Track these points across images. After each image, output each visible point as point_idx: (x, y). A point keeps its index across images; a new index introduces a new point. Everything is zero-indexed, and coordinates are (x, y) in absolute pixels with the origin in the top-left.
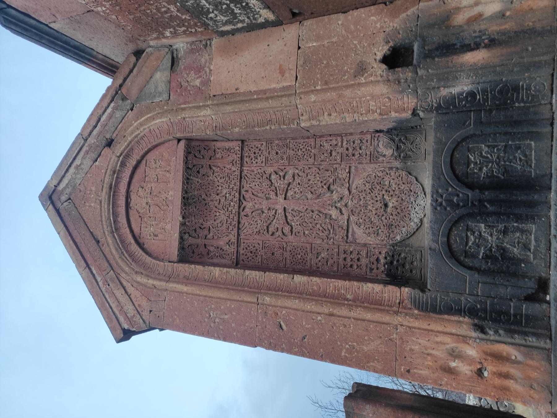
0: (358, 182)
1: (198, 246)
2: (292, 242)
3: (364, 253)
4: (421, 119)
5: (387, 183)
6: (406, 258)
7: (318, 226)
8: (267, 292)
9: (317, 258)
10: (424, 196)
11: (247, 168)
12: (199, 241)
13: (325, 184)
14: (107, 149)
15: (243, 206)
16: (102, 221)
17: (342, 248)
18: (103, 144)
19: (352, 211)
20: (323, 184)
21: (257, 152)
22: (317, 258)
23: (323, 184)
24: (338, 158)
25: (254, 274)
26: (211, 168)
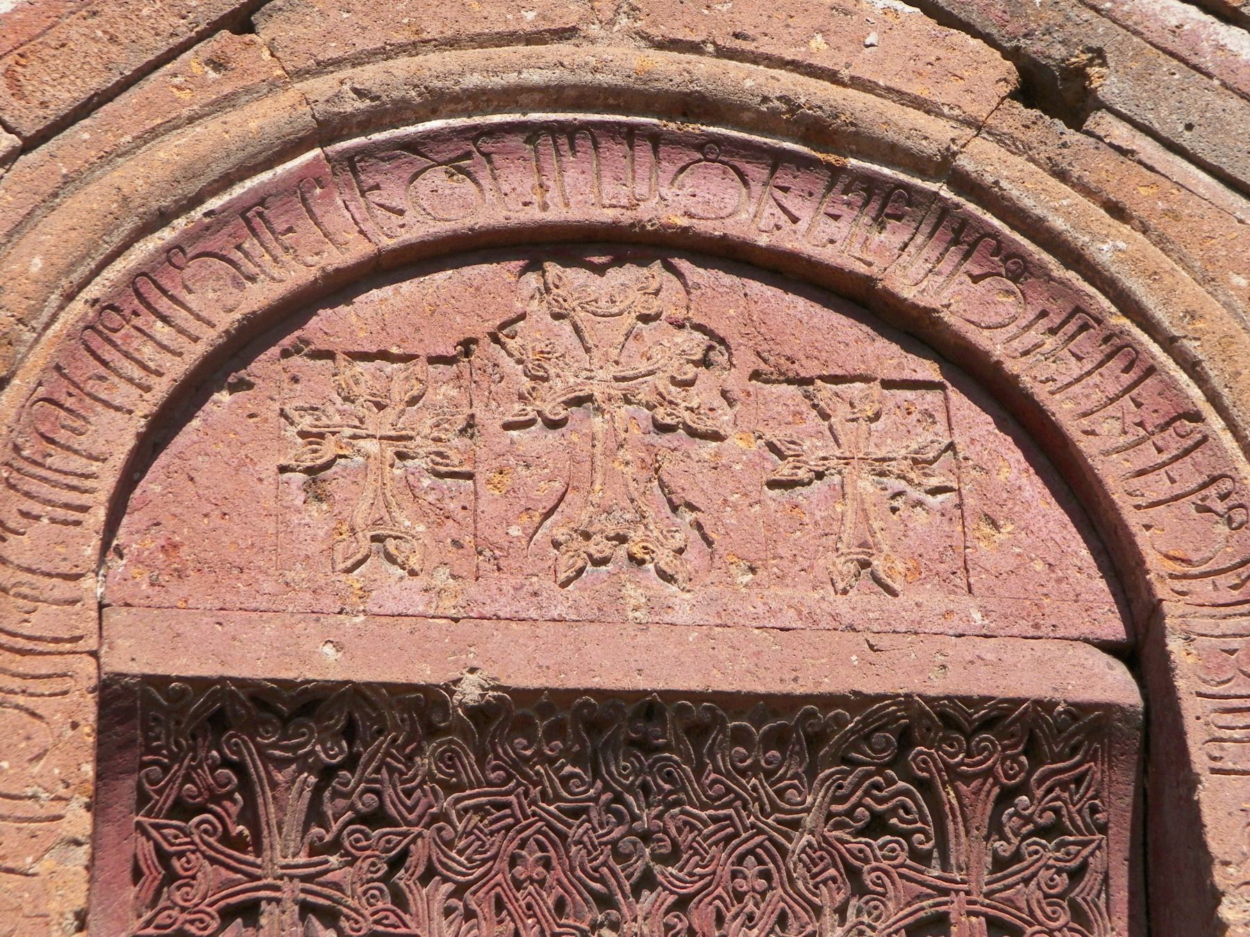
1: (238, 843)
12: (284, 851)
14: (996, 72)
16: (411, 49)
18: (1034, 47)
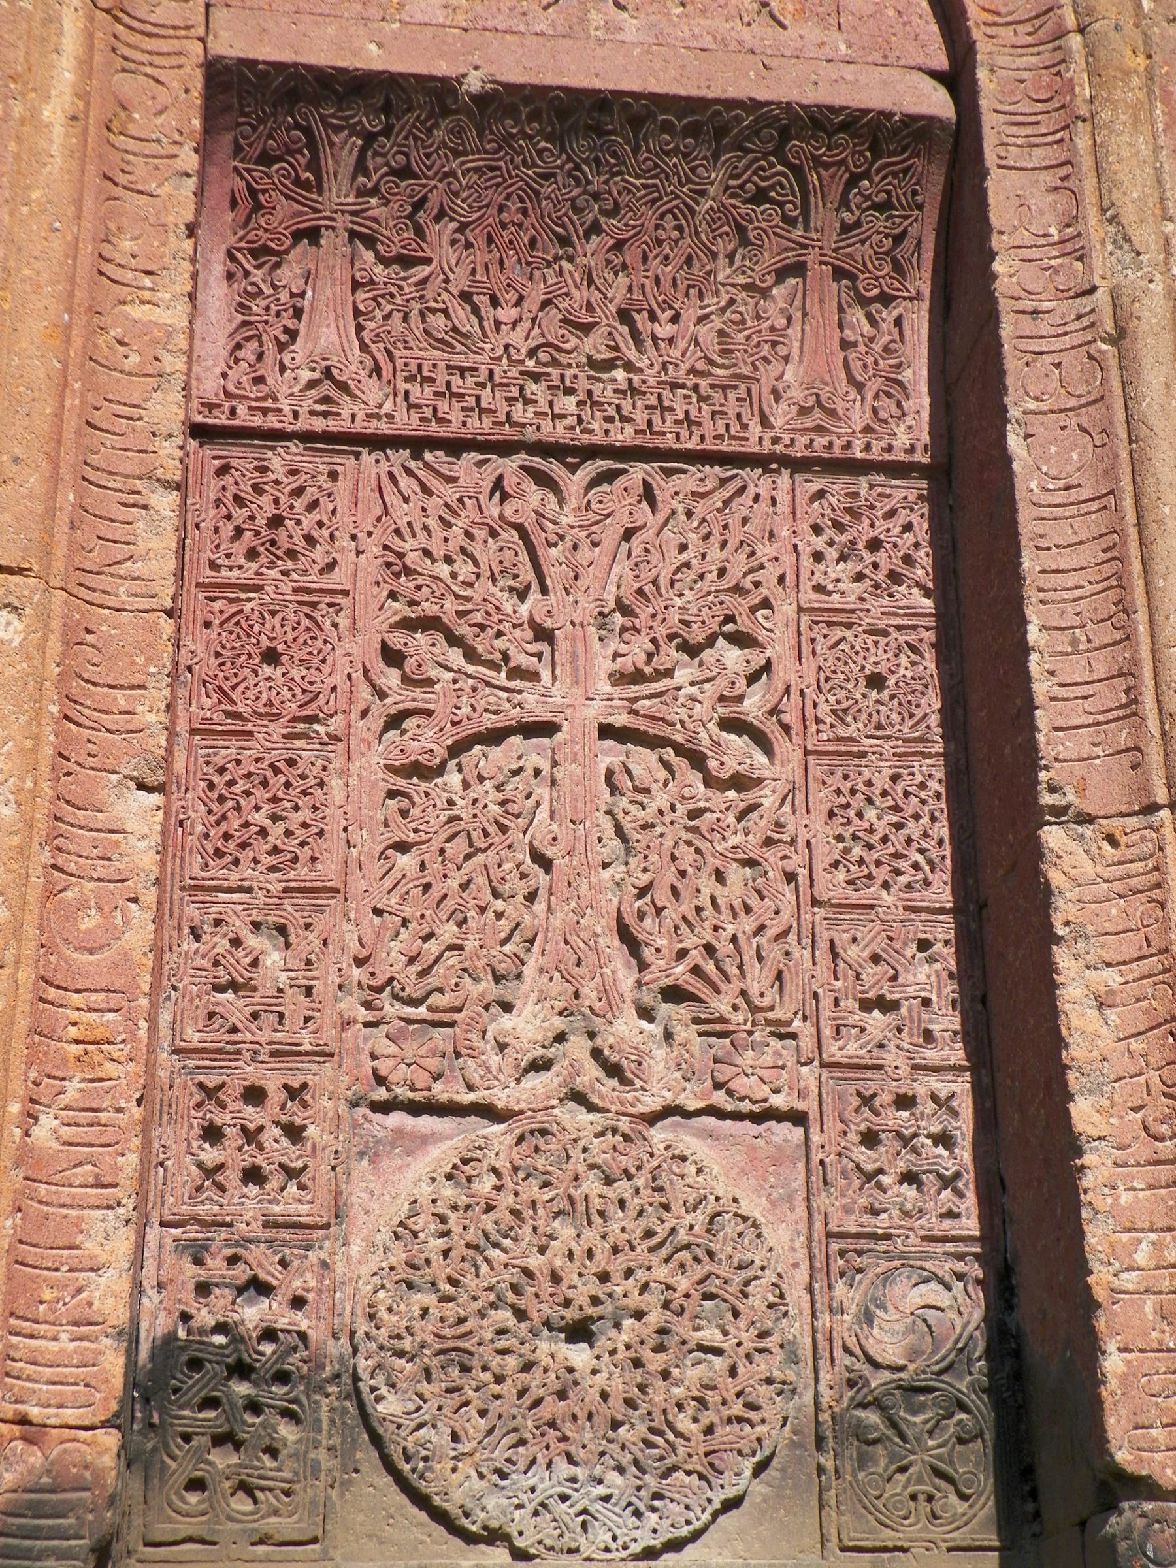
0: (715, 1162)
1: (305, 185)
2: (345, 773)
3: (291, 1203)
4: (1083, 1524)
5: (710, 1335)
6: (273, 1452)
7: (448, 932)
8: (56, 624)
9: (256, 926)
10: (635, 1548)
11: (783, 498)
12: (339, 193)
13: (696, 970)
15: (554, 468)
17: (320, 1075)
19: (544, 1132)
20: (696, 957)
21: (881, 557)
22: (256, 926)
23: (696, 957)
24: (852, 1048)
25: (155, 544)
26: (781, 275)
